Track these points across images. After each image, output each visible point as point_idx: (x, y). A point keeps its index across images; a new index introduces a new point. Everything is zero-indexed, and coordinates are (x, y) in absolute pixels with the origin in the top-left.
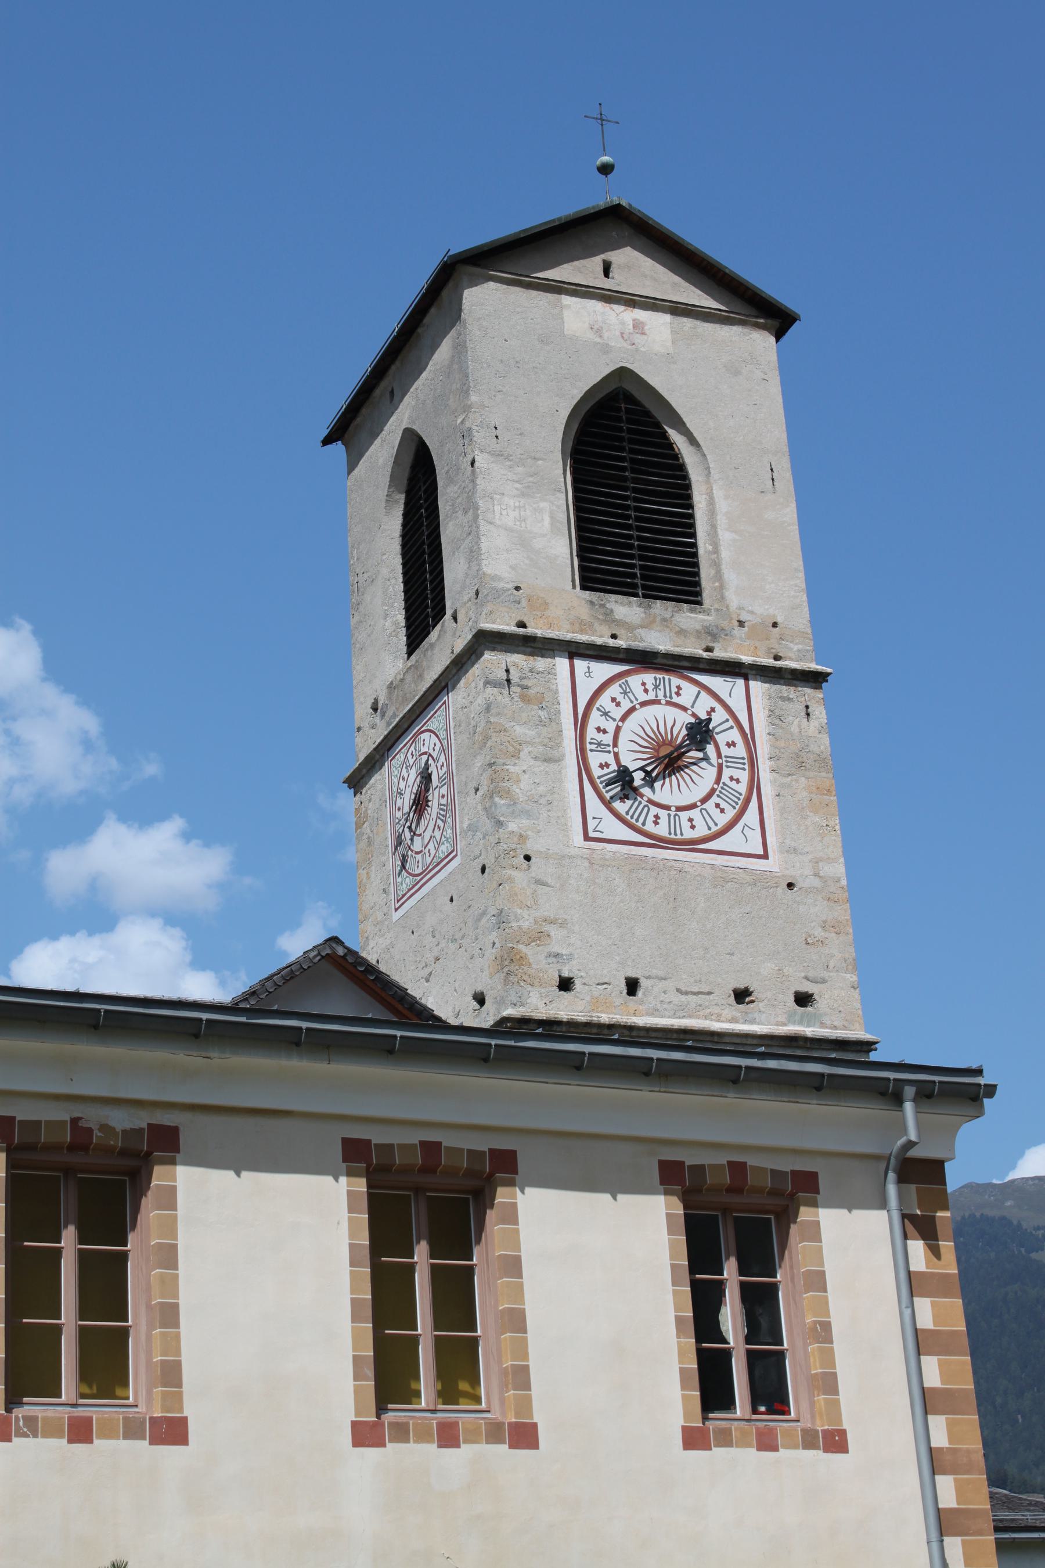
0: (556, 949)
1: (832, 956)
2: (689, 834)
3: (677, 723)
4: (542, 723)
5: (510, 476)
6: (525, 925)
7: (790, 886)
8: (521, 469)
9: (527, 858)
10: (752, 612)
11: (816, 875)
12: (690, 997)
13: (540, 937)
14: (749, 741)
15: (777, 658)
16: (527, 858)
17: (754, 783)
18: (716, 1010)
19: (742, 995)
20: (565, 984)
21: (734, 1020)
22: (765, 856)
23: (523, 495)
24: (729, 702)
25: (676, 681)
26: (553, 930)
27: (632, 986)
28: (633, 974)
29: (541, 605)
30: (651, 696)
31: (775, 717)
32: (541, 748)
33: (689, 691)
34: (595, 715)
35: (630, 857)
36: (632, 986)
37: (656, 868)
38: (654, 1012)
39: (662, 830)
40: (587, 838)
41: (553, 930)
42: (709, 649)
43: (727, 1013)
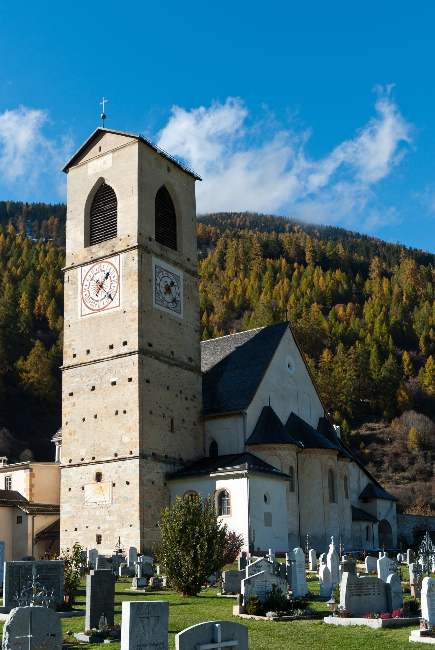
0: (73, 347)
1: (132, 329)
2: (103, 306)
3: (101, 276)
4: (75, 289)
5: (73, 223)
6: (68, 343)
7: (125, 312)
8: (76, 220)
9: (69, 326)
10: (124, 235)
11: (131, 307)
12: (100, 351)
13: (71, 345)
14: (118, 273)
15: (128, 246)
16: (69, 326)
17: (119, 286)
18: (105, 353)
19: (111, 347)
20: (75, 356)
21: (109, 354)
22: (119, 306)
23: (76, 227)
24: (115, 264)
25: (103, 264)
26: (73, 343)
27: (88, 352)
28: (88, 349)
29: (76, 256)
30: (98, 271)
31: (125, 264)
32: (74, 296)
33: (106, 264)
34: (85, 281)
35: (90, 318)
36: (88, 352)
37: (95, 318)
38: (91, 358)
39: (97, 308)
40: (81, 316)
41: (73, 343)
42: (113, 251)
43: (107, 353)
